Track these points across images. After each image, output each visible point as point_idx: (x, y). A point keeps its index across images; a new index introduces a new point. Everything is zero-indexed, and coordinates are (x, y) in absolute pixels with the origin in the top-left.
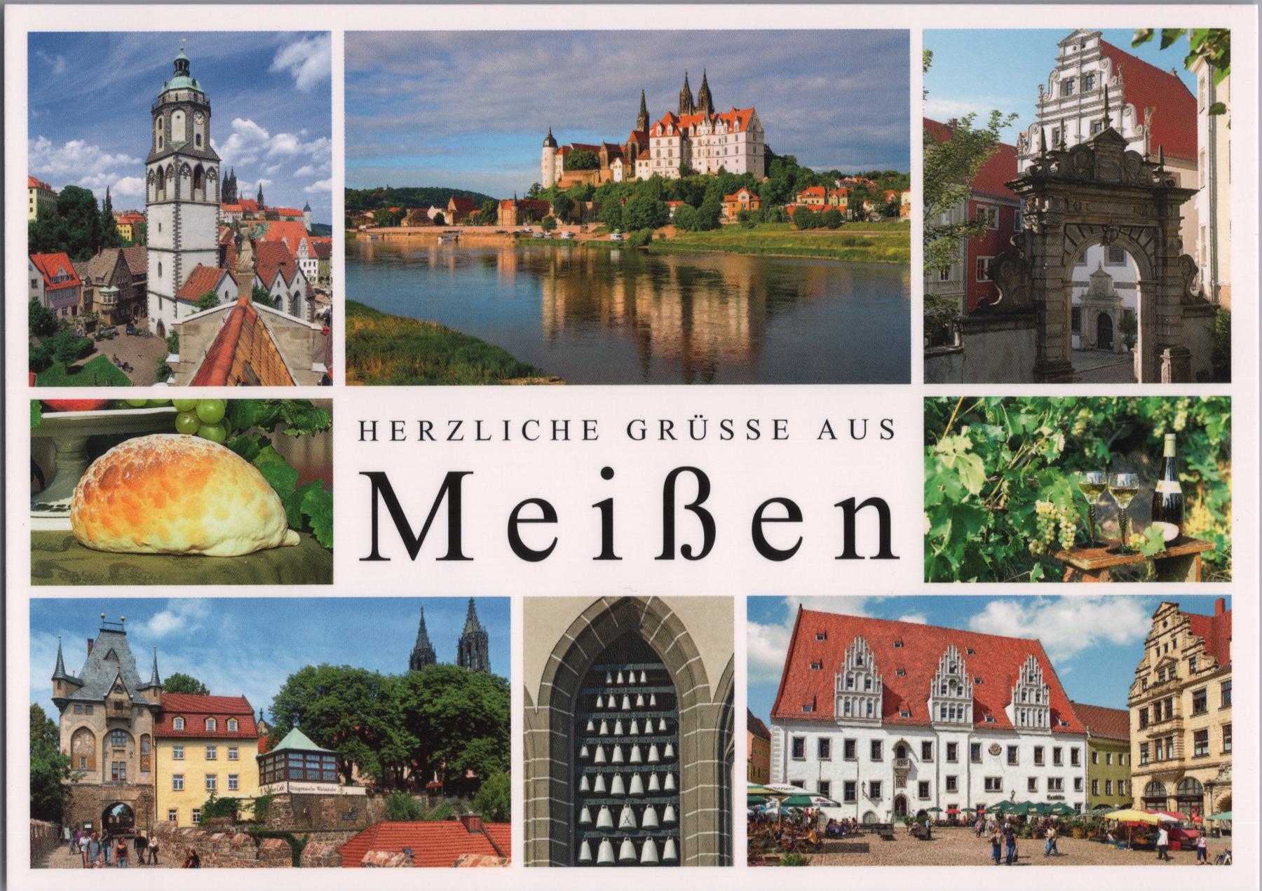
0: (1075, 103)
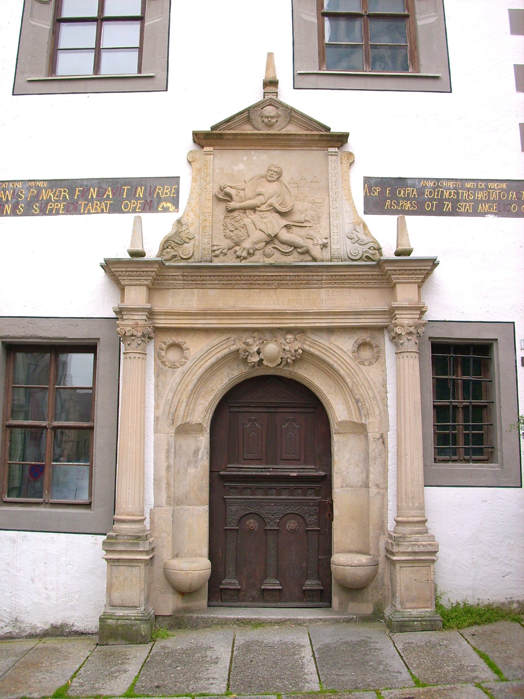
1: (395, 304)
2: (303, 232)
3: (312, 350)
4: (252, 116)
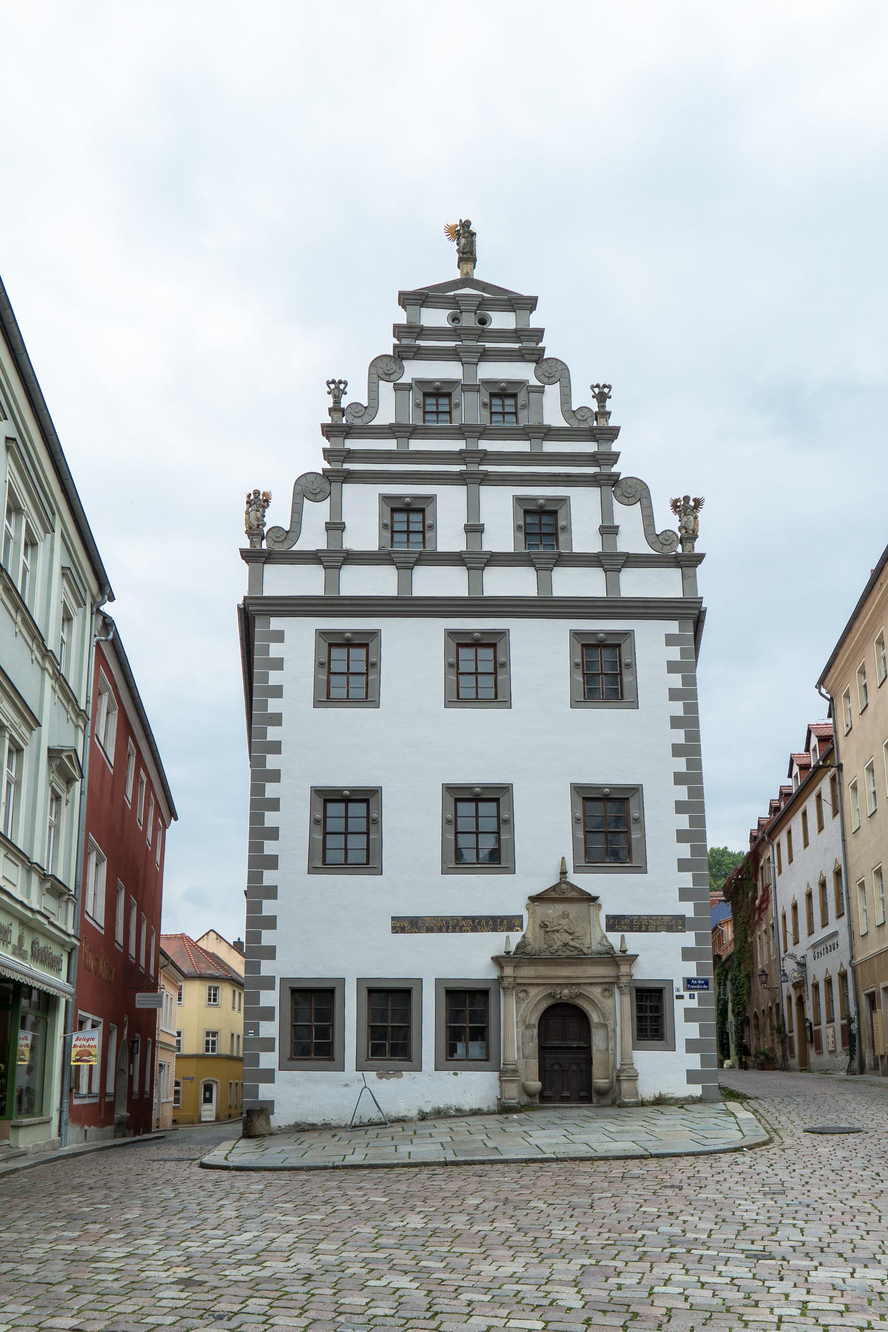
2: (579, 941)
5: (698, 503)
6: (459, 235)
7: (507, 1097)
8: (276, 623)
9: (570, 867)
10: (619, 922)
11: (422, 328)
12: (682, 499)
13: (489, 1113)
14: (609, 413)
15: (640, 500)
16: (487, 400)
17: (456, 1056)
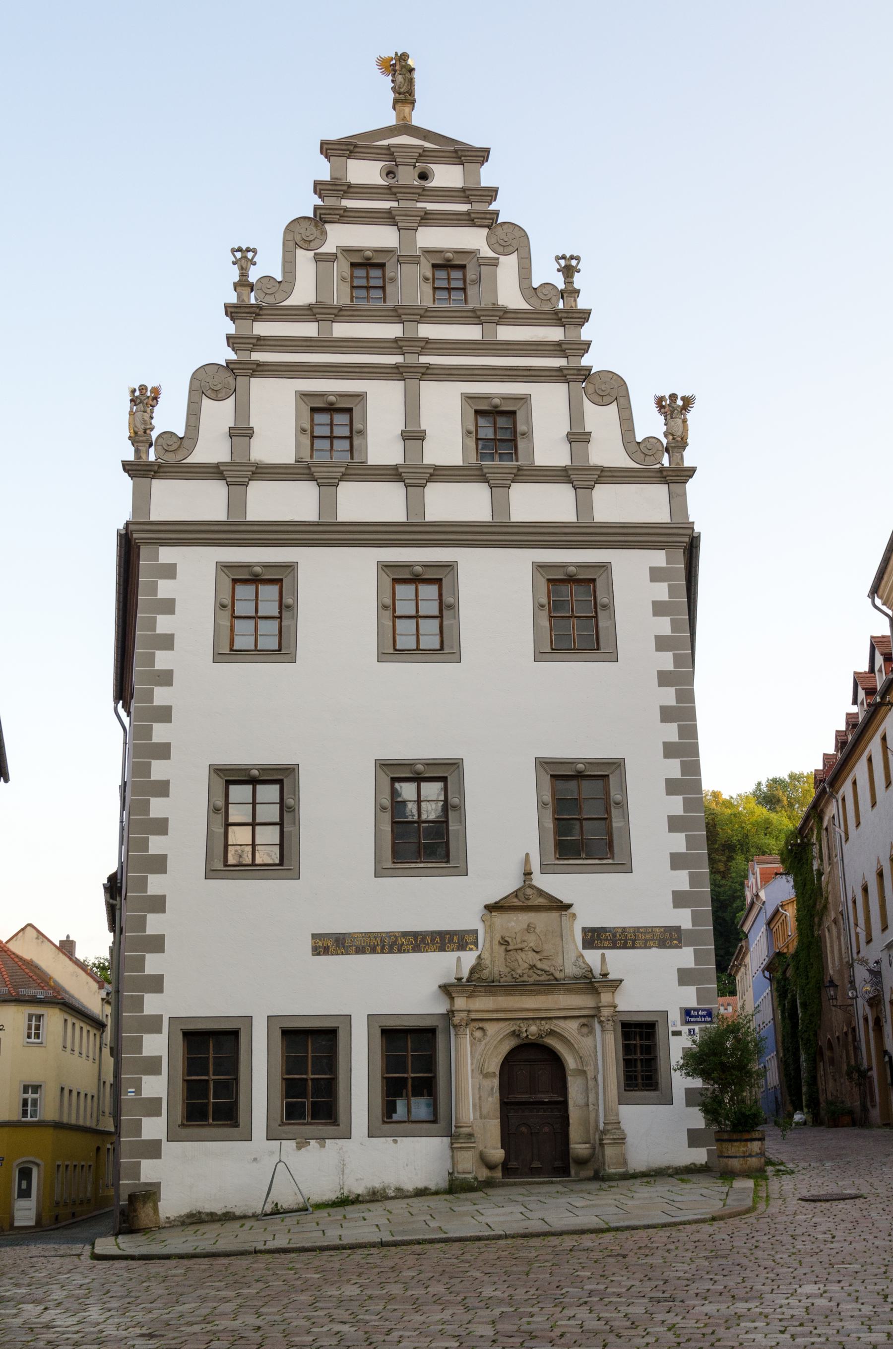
0: (392, 331)
1: (600, 1005)
3: (555, 1029)
4: (519, 894)
5: (688, 402)
6: (395, 71)
7: (460, 1170)
8: (166, 555)
9: (535, 866)
10: (598, 936)
11: (350, 186)
12: (667, 397)
13: (436, 1193)
14: (578, 292)
15: (616, 399)
16: (429, 274)
17: (395, 1117)
